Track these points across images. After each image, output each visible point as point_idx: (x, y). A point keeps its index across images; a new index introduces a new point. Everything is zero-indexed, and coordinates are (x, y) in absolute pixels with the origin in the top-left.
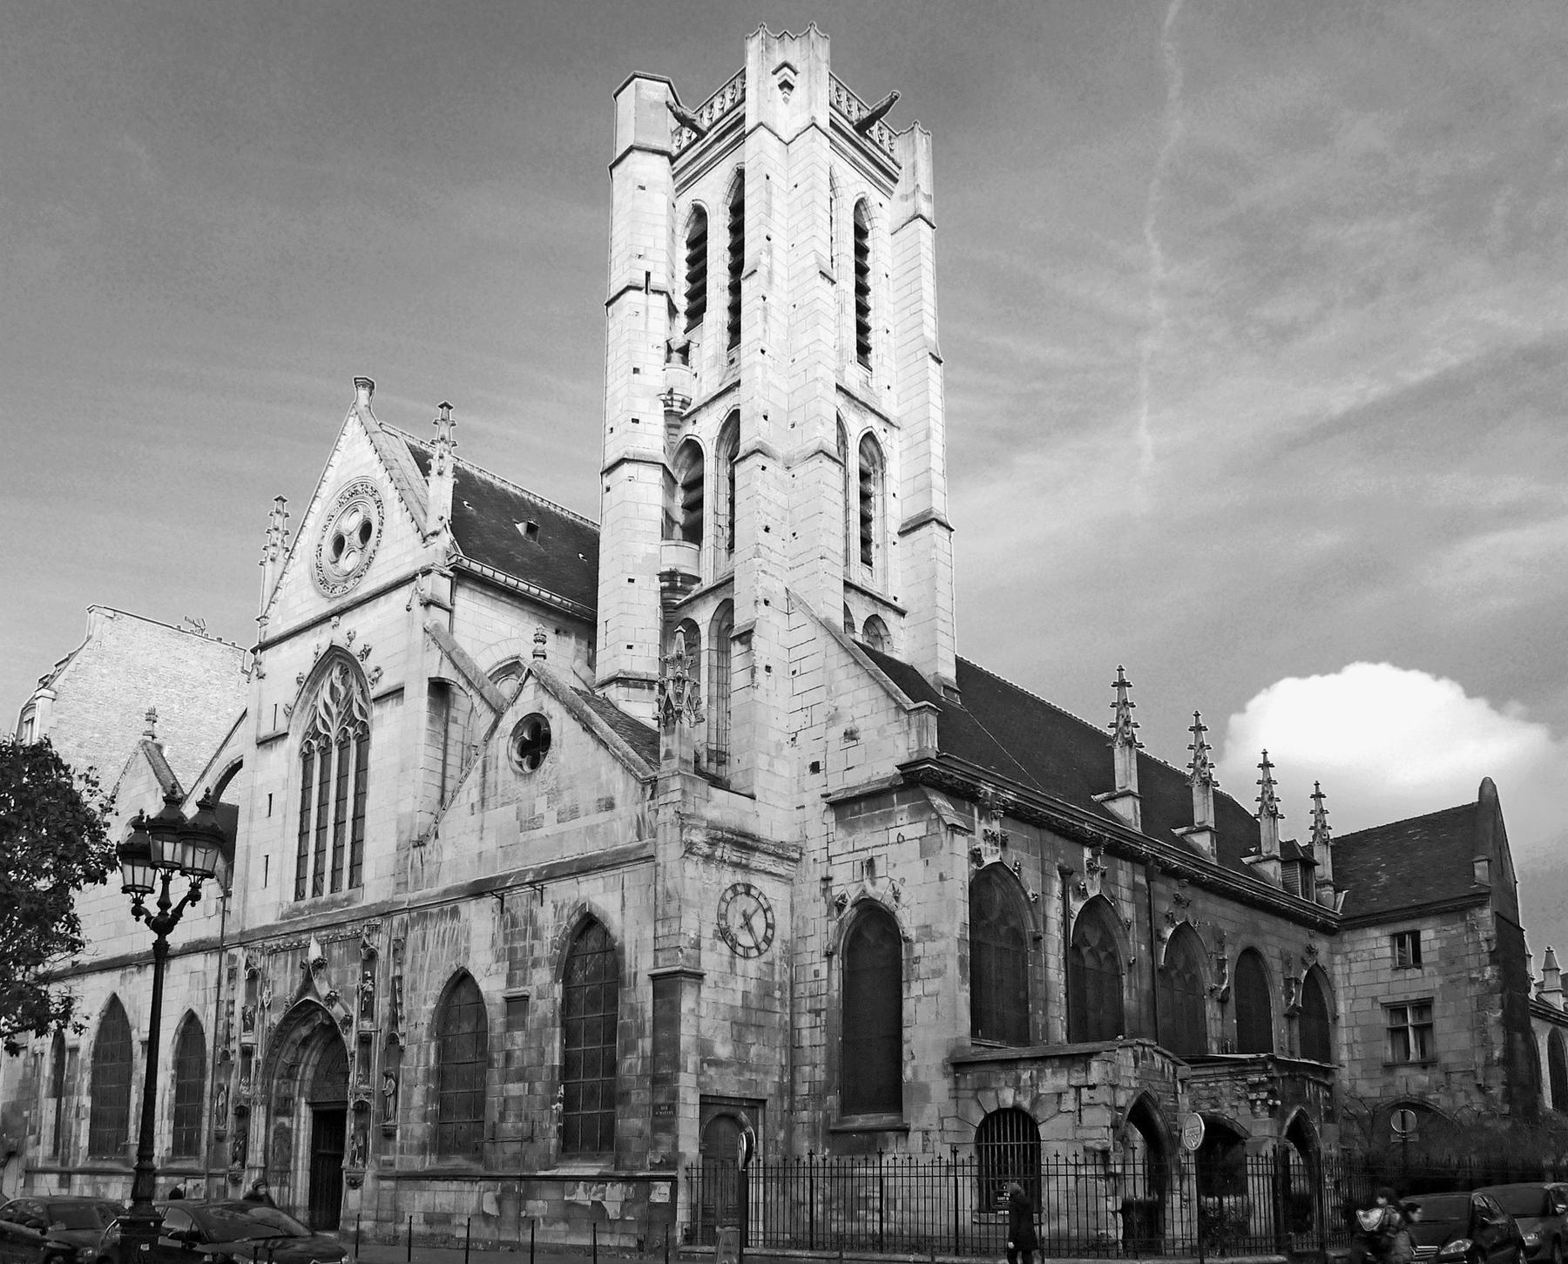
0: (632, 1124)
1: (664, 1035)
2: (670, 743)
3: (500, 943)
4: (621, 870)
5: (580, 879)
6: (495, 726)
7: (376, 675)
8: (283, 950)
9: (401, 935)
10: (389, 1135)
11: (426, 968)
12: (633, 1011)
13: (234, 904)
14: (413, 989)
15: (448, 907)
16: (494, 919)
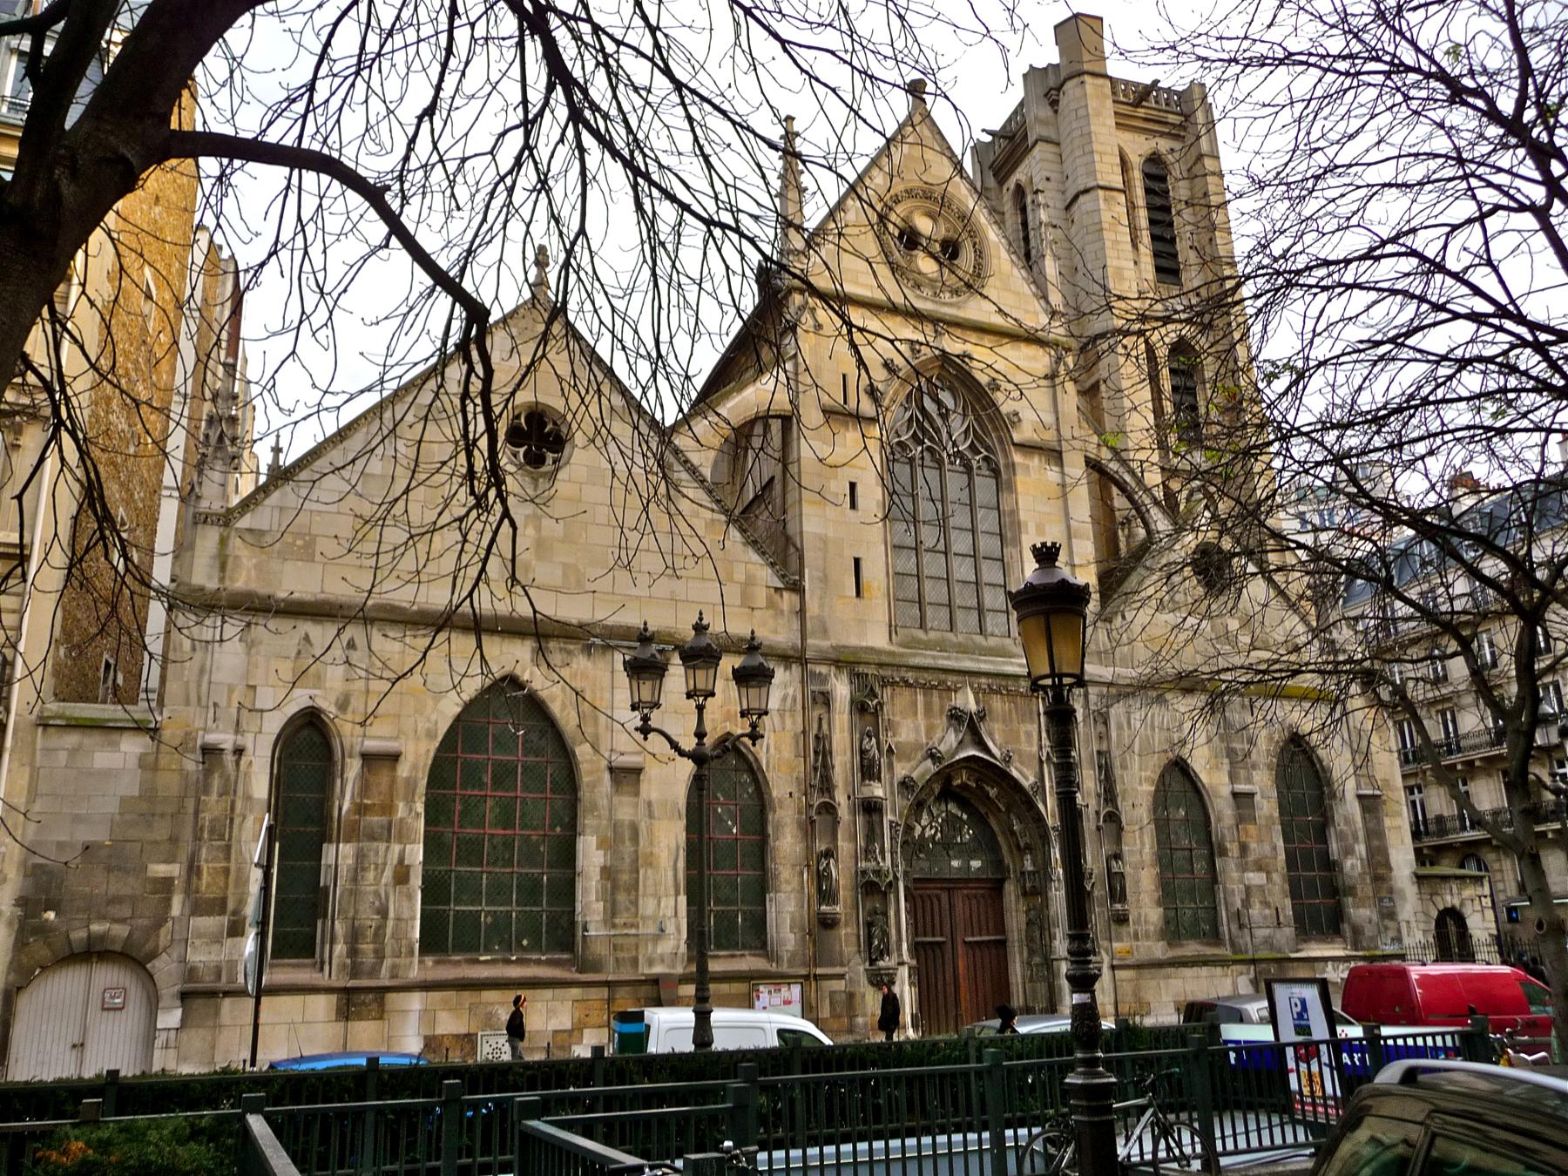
0: (1361, 913)
1: (1376, 843)
10: (1122, 919)
11: (1137, 747)
12: (1348, 821)
14: (1124, 767)
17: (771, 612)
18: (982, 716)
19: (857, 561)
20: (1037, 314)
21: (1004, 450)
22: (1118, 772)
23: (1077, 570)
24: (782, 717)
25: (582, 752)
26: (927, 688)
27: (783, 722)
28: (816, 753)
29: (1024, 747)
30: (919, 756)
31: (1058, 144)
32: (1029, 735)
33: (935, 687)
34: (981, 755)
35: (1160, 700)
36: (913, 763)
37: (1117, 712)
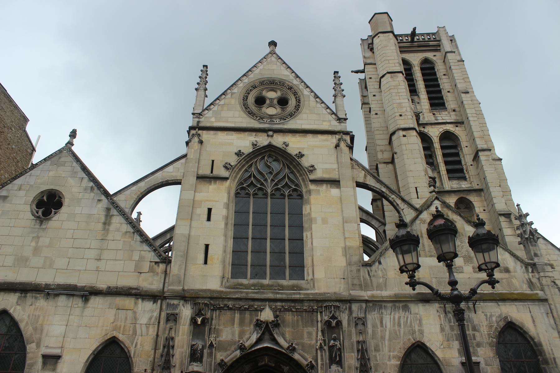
2: (535, 250)
3: (447, 328)
4: (526, 303)
5: (500, 304)
6: (417, 217)
7: (311, 169)
8: (230, 309)
9: (362, 315)
11: (387, 337)
13: (175, 268)
14: (377, 349)
15: (401, 305)
16: (439, 316)
17: (151, 274)
18: (276, 325)
19: (207, 246)
20: (330, 121)
21: (305, 185)
22: (372, 353)
23: (347, 240)
24: (148, 328)
25: (31, 347)
26: (241, 310)
27: (148, 331)
28: (164, 347)
29: (306, 341)
30: (233, 348)
31: (375, 64)
32: (310, 334)
33: (246, 309)
34: (275, 347)
35: (406, 308)
36: (229, 352)
37: (372, 317)
